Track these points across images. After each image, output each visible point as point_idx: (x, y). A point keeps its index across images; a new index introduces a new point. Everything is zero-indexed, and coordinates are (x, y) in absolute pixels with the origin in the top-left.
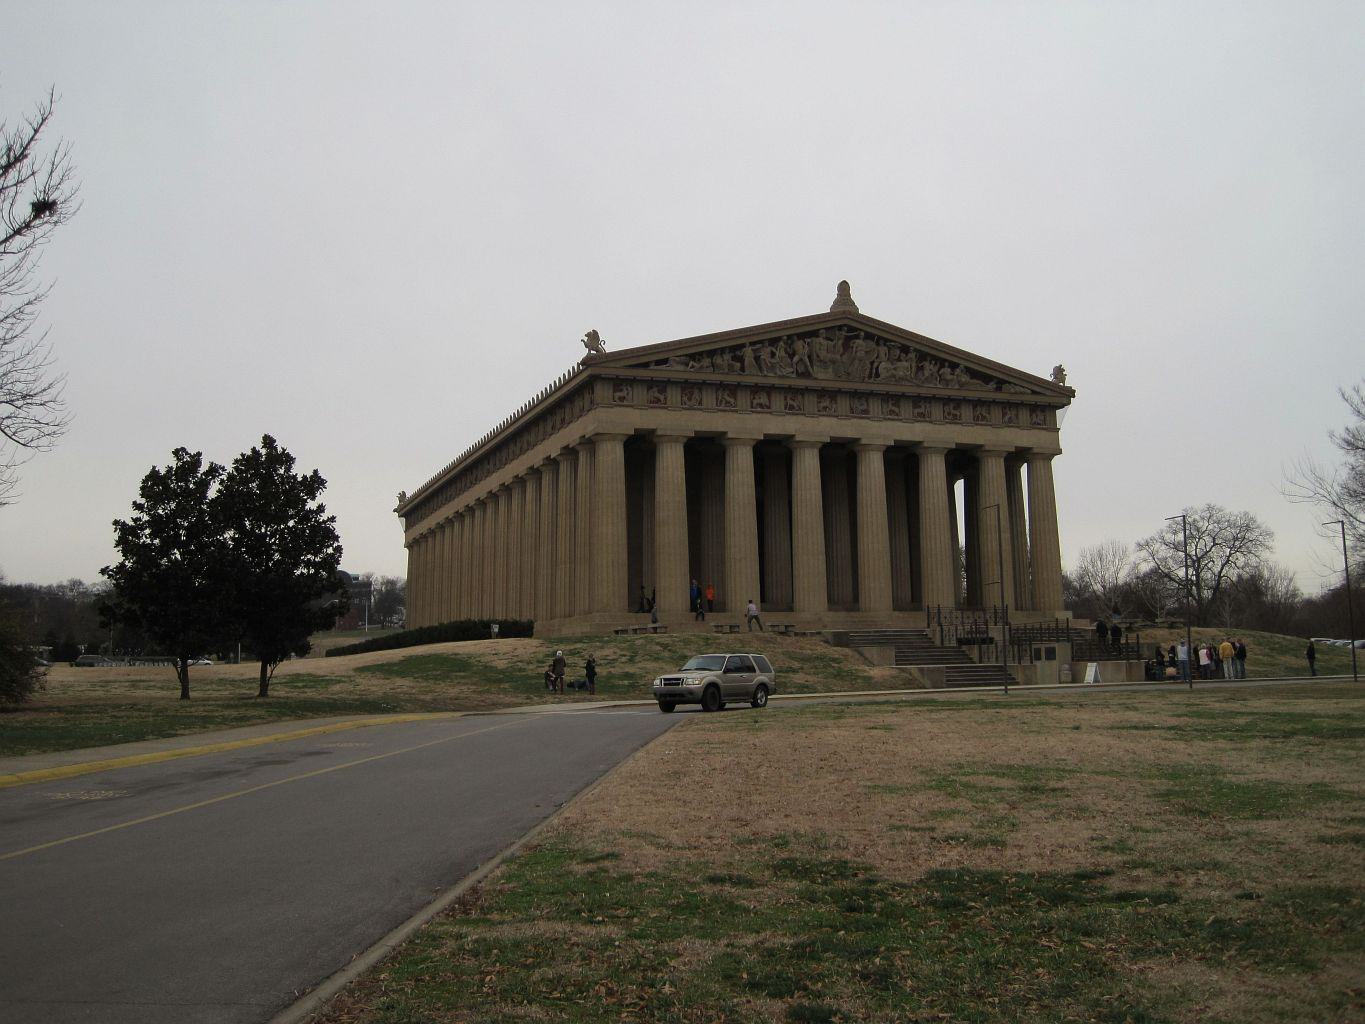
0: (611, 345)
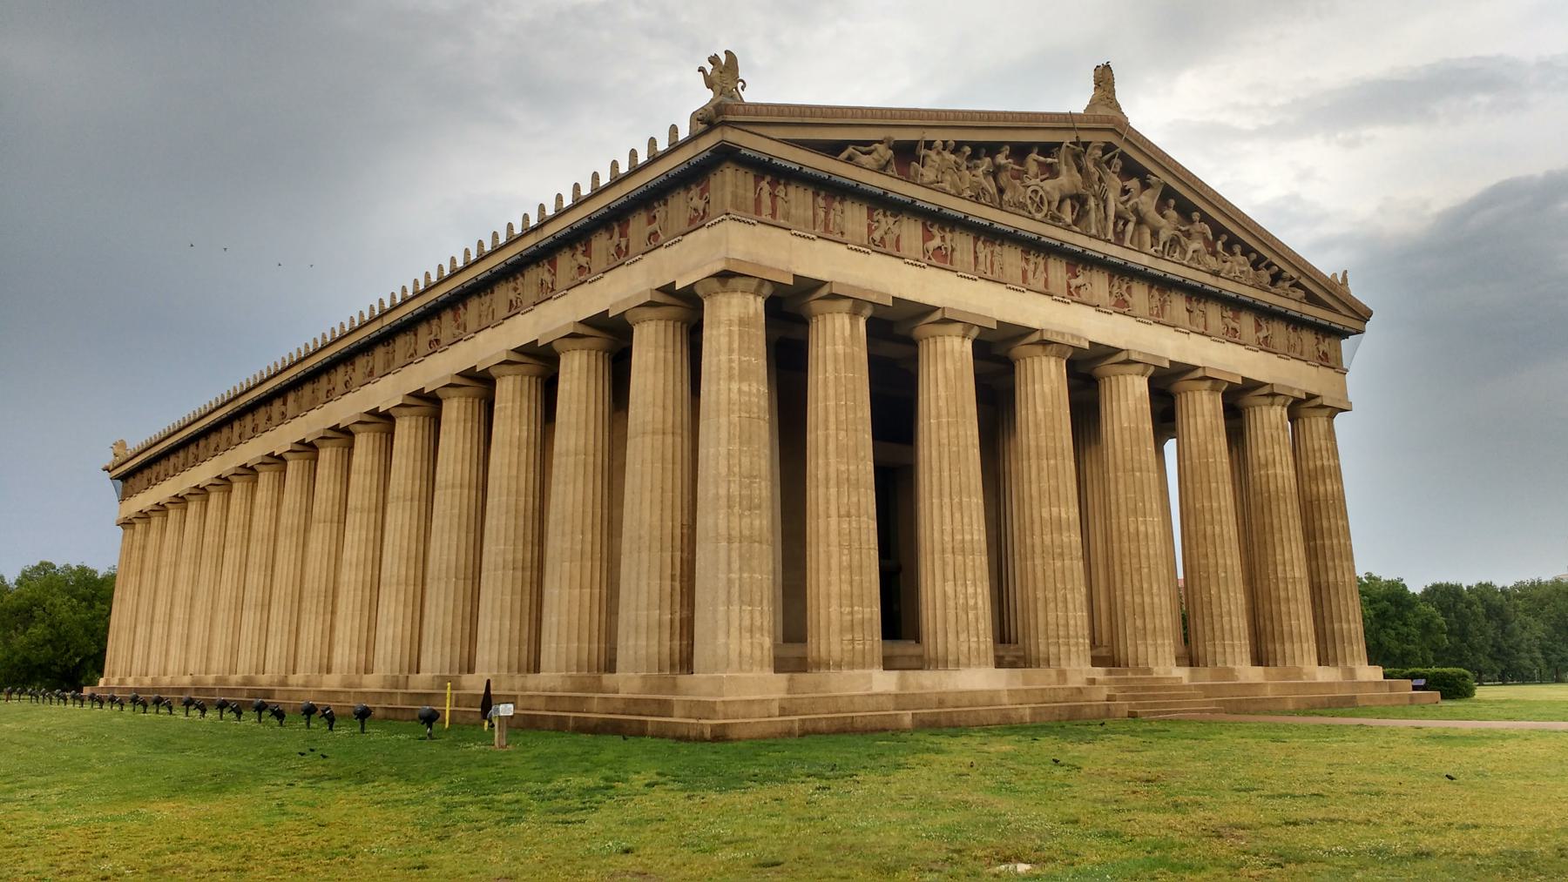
0: (756, 91)
